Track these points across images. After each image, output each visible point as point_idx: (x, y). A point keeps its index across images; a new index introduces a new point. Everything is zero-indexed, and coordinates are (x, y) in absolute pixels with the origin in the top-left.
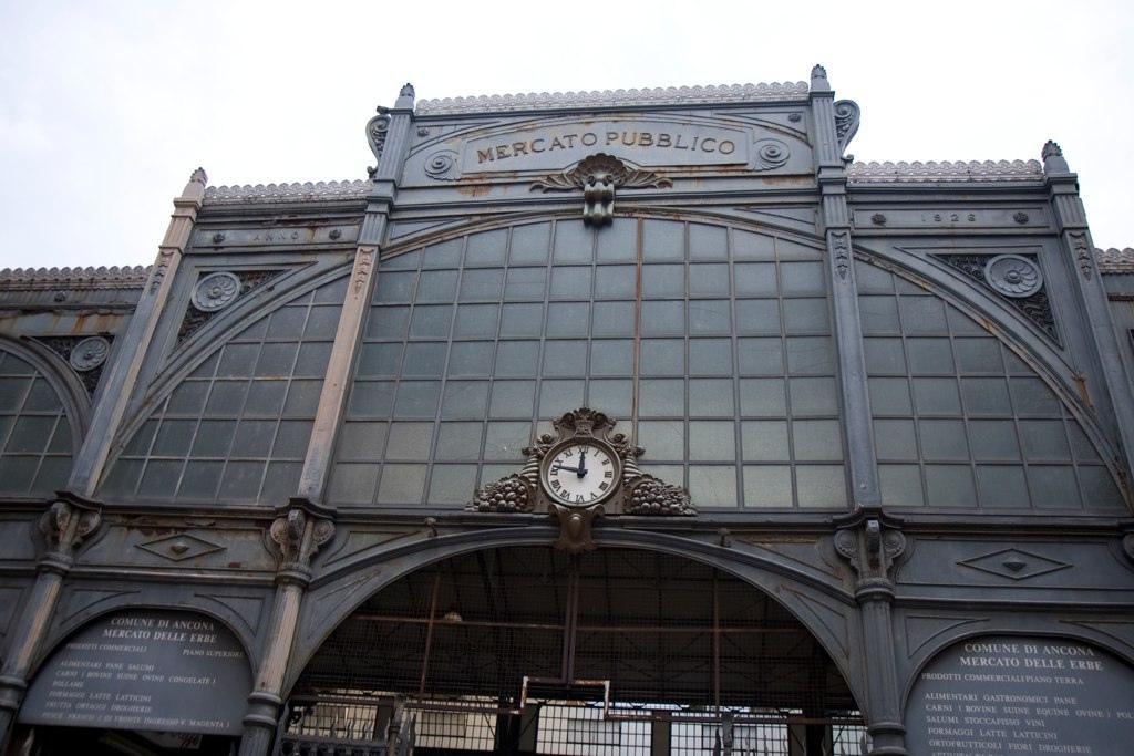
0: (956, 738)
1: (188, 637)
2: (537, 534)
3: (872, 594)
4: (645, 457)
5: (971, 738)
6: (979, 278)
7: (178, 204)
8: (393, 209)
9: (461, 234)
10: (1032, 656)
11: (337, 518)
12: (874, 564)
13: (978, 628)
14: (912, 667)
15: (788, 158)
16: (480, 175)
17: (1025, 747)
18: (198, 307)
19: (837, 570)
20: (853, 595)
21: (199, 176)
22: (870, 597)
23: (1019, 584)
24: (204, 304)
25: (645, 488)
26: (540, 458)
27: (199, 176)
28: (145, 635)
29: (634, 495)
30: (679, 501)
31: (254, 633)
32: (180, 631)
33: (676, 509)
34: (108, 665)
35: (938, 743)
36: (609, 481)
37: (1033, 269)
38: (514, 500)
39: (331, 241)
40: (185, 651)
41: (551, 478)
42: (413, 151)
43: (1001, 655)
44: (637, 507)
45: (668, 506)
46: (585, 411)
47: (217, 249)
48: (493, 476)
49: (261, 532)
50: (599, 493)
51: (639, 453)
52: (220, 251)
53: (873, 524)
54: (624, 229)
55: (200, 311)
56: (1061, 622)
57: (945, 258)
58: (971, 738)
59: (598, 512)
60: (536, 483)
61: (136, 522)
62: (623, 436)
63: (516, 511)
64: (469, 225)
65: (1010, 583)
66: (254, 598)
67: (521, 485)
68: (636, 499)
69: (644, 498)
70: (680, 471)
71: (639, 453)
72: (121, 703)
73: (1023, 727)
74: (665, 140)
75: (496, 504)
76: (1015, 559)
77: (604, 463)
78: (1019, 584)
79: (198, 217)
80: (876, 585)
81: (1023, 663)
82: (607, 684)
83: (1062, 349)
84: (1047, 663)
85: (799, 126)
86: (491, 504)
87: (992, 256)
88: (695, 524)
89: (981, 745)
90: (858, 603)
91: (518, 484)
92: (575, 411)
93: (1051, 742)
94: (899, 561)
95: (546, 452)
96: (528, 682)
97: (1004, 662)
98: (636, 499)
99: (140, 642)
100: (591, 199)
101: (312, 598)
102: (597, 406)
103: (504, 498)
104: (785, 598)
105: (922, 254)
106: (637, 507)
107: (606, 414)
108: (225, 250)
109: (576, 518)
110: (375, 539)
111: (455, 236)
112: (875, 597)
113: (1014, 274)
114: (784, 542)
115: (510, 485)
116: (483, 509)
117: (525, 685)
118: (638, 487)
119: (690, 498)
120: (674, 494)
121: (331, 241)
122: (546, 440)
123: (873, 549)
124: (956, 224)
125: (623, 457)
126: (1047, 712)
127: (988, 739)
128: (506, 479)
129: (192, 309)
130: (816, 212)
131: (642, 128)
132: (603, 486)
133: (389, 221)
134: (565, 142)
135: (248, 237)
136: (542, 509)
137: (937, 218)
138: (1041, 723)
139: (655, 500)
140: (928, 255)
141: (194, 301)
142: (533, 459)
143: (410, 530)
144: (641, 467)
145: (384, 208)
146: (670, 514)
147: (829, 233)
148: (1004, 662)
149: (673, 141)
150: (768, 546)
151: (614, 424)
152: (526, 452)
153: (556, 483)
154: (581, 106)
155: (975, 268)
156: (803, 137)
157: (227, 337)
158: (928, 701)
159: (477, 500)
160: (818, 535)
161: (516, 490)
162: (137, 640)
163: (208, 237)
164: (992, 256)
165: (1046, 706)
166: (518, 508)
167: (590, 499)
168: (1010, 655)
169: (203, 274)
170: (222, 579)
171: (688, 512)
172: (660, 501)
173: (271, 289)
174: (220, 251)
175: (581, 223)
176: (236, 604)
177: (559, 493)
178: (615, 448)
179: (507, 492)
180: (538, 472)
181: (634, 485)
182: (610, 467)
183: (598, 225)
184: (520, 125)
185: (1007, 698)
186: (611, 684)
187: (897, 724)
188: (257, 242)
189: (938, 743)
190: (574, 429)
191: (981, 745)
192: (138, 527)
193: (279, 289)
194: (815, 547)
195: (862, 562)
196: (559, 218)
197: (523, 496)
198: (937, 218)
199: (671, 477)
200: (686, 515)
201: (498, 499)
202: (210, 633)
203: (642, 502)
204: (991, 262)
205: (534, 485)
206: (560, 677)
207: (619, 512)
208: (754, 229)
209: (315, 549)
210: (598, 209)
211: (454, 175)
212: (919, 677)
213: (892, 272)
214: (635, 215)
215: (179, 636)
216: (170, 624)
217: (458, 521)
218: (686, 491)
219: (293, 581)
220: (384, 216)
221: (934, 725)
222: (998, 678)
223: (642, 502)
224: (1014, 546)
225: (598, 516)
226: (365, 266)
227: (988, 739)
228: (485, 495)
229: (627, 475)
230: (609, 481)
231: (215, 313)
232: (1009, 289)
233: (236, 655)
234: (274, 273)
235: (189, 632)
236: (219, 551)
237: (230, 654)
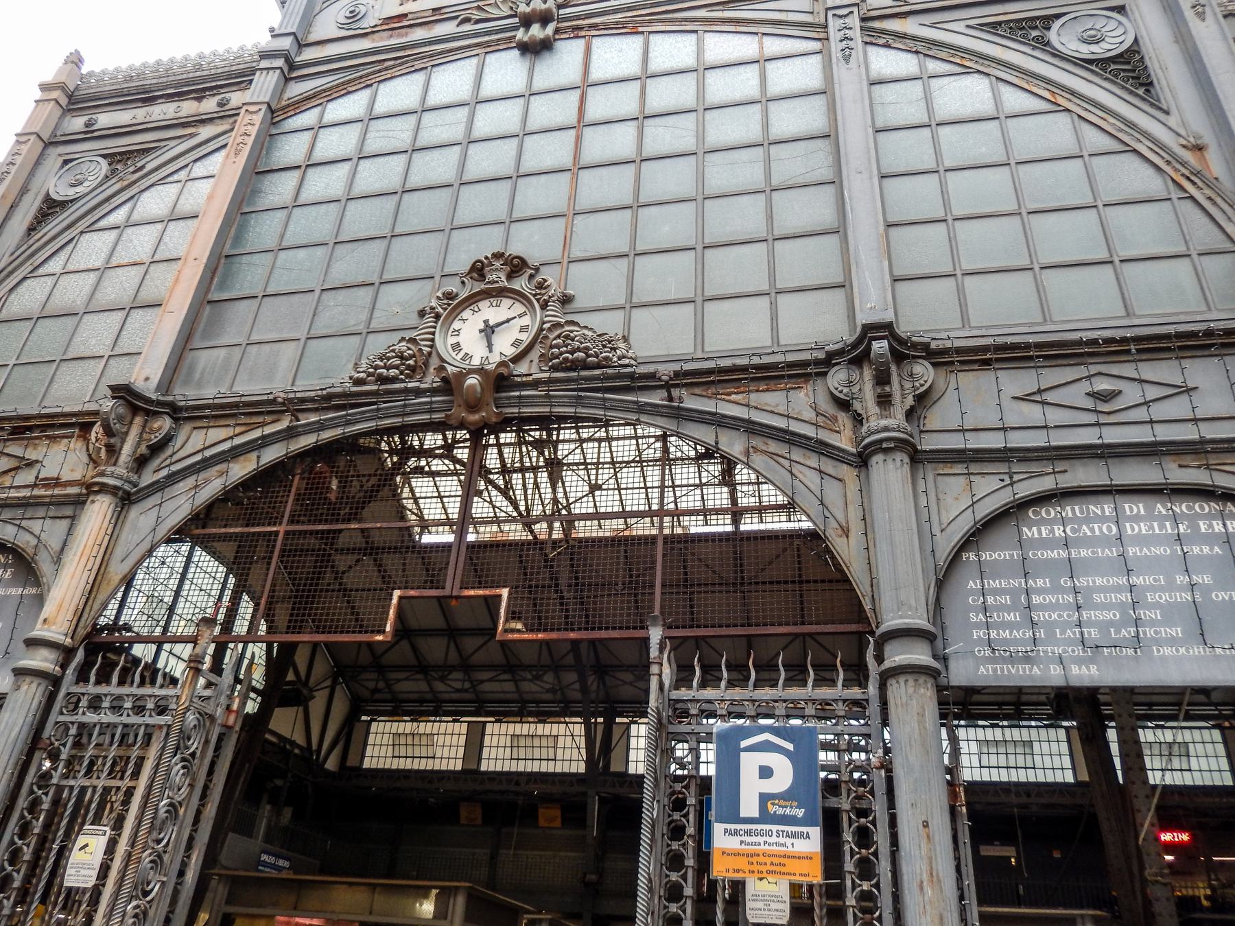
3: (881, 441)
6: (1043, 44)
7: (45, 87)
8: (292, 66)
9: (369, 83)
10: (1136, 518)
11: (176, 412)
12: (884, 401)
13: (1046, 484)
14: (946, 545)
20: (854, 450)
21: (75, 60)
22: (878, 447)
23: (1112, 419)
24: (61, 191)
27: (75, 60)
33: (606, 358)
37: (1120, 23)
38: (397, 367)
43: (1088, 520)
47: (90, 134)
48: (378, 345)
51: (566, 300)
53: (880, 347)
54: (569, 53)
55: (55, 201)
56: (1180, 466)
57: (993, 27)
65: (1092, 418)
67: (409, 349)
76: (1103, 385)
78: (1112, 419)
79: (70, 103)
80: (886, 429)
82: (505, 592)
83: (1167, 113)
84: (1162, 527)
87: (1058, 16)
88: (631, 376)
90: (862, 460)
92: (486, 258)
93: (1172, 641)
94: (923, 399)
96: (400, 598)
97: (1092, 530)
98: (556, 350)
100: (526, 22)
102: (515, 249)
108: (96, 134)
110: (222, 433)
111: (363, 85)
112: (884, 445)
113: (1092, 32)
116: (358, 382)
117: (395, 601)
120: (609, 344)
123: (882, 379)
126: (1165, 597)
135: (123, 117)
136: (431, 379)
139: (579, 349)
140: (968, 26)
142: (429, 319)
143: (268, 418)
145: (280, 63)
147: (830, 14)
148: (1092, 530)
150: (733, 397)
151: (537, 270)
152: (422, 314)
153: (457, 347)
155: (1034, 33)
157: (82, 225)
160: (807, 377)
163: (77, 123)
164: (1058, 16)
165: (1162, 589)
168: (1103, 519)
169: (66, 162)
173: (143, 167)
175: (516, 52)
178: (534, 295)
181: (552, 336)
183: (535, 50)
185: (1099, 581)
186: (510, 593)
187: (921, 622)
188: (134, 121)
193: (149, 167)
195: (867, 403)
196: (488, 50)
197: (411, 362)
199: (609, 324)
203: (561, 354)
204: (1057, 24)
206: (443, 588)
208: (732, 29)
209: (143, 449)
210: (536, 31)
211: (368, 23)
212: (955, 559)
213: (917, 52)
214: (582, 33)
217: (328, 401)
218: (625, 339)
219: (104, 489)
220: (278, 71)
223: (561, 354)
226: (249, 127)
228: (363, 367)
231: (71, 201)
232: (1085, 50)
236: (30, 464)
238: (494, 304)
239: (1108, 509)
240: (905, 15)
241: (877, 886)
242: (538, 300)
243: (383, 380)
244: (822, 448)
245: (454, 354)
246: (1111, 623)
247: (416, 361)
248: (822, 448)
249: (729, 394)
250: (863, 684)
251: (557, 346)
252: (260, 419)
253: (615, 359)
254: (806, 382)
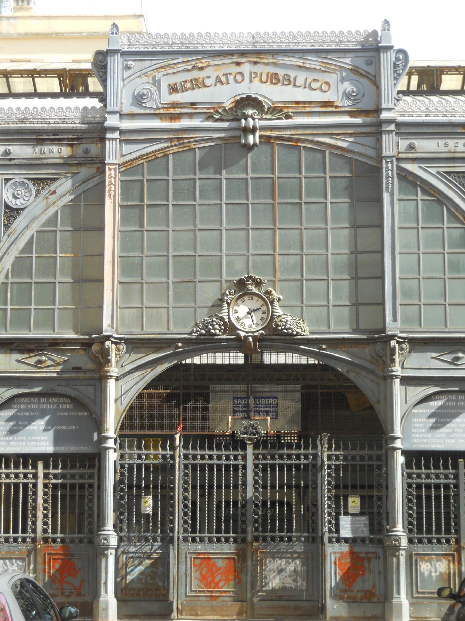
0: (424, 438)
1: (58, 406)
5: (430, 438)
15: (363, 96)
16: (175, 105)
17: (453, 441)
18: (10, 204)
19: (377, 361)
24: (13, 203)
28: (36, 406)
31: (94, 402)
32: (53, 403)
34: (20, 423)
35: (416, 441)
36: (265, 316)
39: (85, 156)
40: (58, 414)
42: (126, 81)
49: (85, 349)
52: (13, 162)
58: (430, 438)
61: (13, 346)
64: (171, 146)
66: (90, 385)
72: (32, 441)
73: (453, 432)
74: (288, 81)
81: (457, 404)
85: (370, 69)
89: (434, 441)
99: (33, 410)
101: (120, 382)
104: (351, 376)
105: (433, 171)
108: (16, 162)
114: (352, 347)
117: (230, 420)
121: (85, 156)
124: (458, 150)
127: (438, 438)
129: (7, 206)
130: (377, 139)
131: (272, 70)
133: (120, 141)
134: (223, 79)
137: (446, 145)
138: (461, 430)
140: (438, 173)
141: (7, 201)
149: (292, 79)
154: (234, 48)
156: (373, 78)
158: (414, 423)
162: (31, 409)
168: (452, 400)
169: (7, 180)
170: (71, 377)
174: (13, 162)
176: (82, 388)
184: (194, 62)
186: (271, 418)
189: (416, 441)
191: (434, 441)
192: (16, 350)
194: (367, 350)
196: (226, 142)
198: (446, 145)
202: (69, 403)
215: (53, 406)
216: (47, 400)
221: (415, 433)
222: (446, 411)
224: (460, 347)
227: (438, 438)
230: (265, 316)
231: (23, 209)
233: (86, 414)
234: (55, 180)
235: (58, 404)
237: (82, 414)
238: (250, 298)
239: (454, 397)
240: (414, 160)
241: (382, 503)
244: (372, 372)
246: (449, 433)
248: (372, 372)
249: (342, 348)
250: (382, 450)
252: (162, 345)
254: (368, 345)
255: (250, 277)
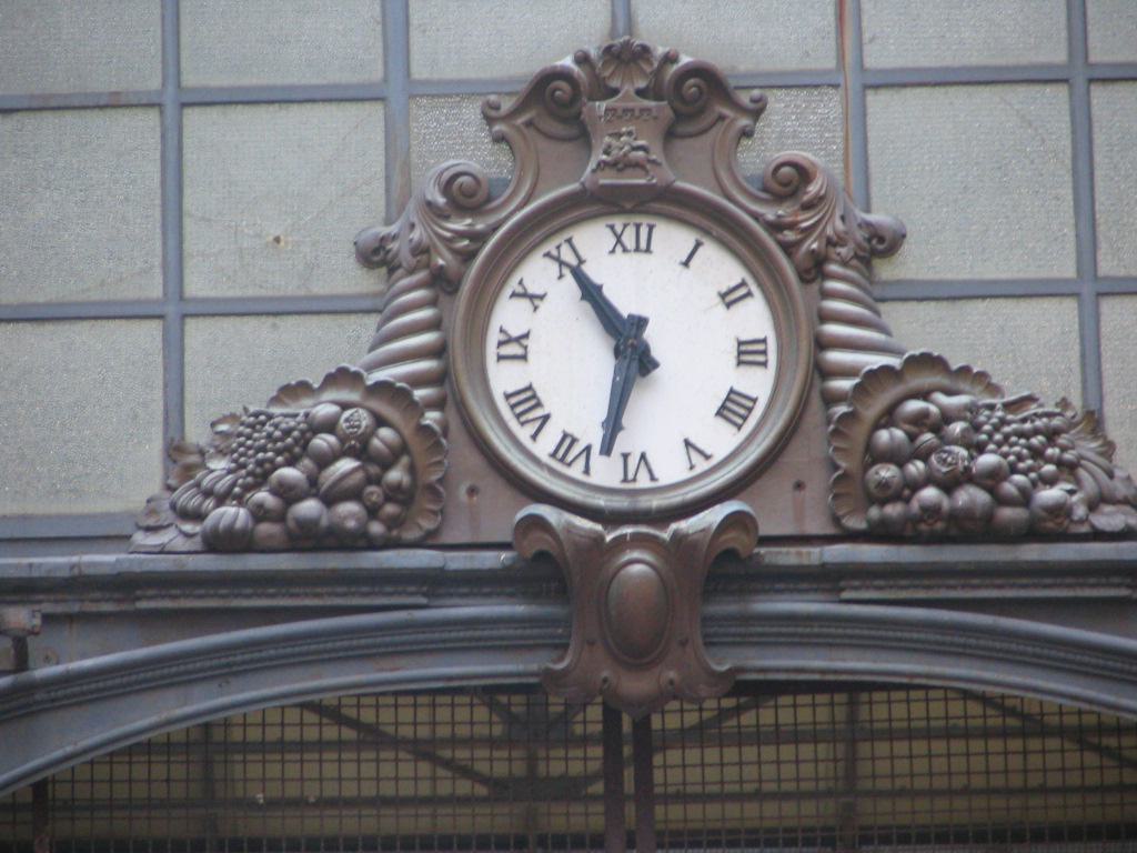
2: (472, 638)
4: (906, 266)
25: (920, 420)
26: (442, 283)
29: (876, 456)
30: (1069, 469)
33: (1060, 510)
36: (758, 384)
38: (355, 494)
41: (504, 378)
44: (893, 510)
45: (1025, 498)
46: (626, 55)
50: (721, 440)
51: (882, 244)
59: (734, 539)
60: (438, 404)
62: (804, 174)
63: (373, 545)
67: (380, 421)
68: (887, 472)
69: (915, 469)
70: (1061, 316)
71: (882, 244)
75: (280, 517)
77: (729, 298)
86: (259, 514)
91: (364, 419)
92: (583, 59)
95: (468, 257)
98: (887, 472)
103: (313, 487)
106: (893, 510)
107: (720, 61)
109: (638, 567)
115: (329, 426)
116: (220, 542)
118: (889, 418)
119: (1108, 449)
122: (464, 196)
125: (814, 270)
128: (300, 389)
132: (732, 407)
144: (893, 314)
146: (1034, 532)
151: (757, 111)
152: (374, 256)
153: (526, 400)
159: (188, 498)
161: (359, 448)
166: (376, 528)
167: (683, 474)
171: (1111, 519)
172: (991, 480)
177: (544, 447)
179: (324, 461)
180: (438, 351)
181: (872, 410)
182: (755, 318)
190: (583, 137)
197: (395, 475)
200: (1098, 535)
201: (288, 494)
205: (431, 417)
207: (816, 526)
218: (1093, 422)
223: (915, 486)
225: (730, 554)
229: (835, 357)
238: (629, 238)
242: (788, 248)
243: (308, 538)
245: (523, 434)
247: (412, 470)
251: (897, 457)
253: (1080, 511)
255: (626, 55)
